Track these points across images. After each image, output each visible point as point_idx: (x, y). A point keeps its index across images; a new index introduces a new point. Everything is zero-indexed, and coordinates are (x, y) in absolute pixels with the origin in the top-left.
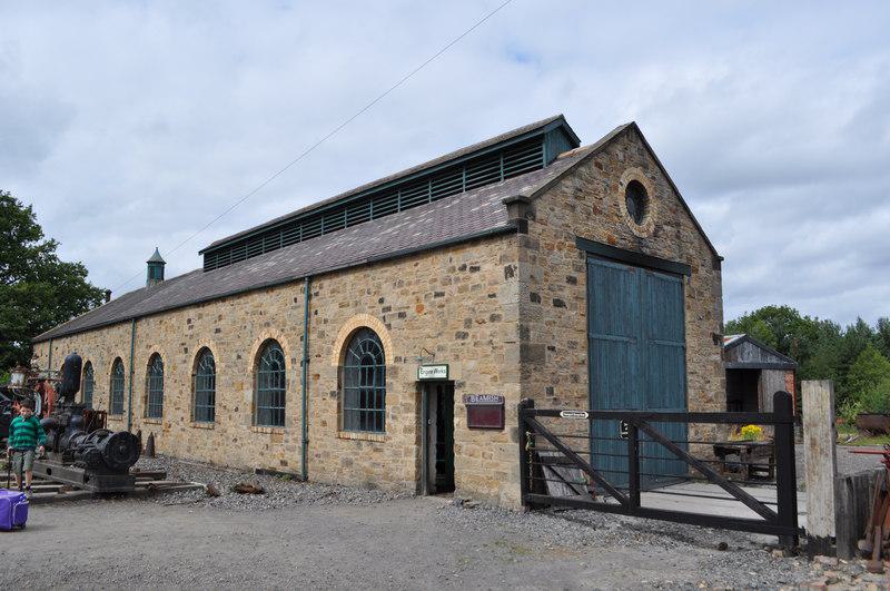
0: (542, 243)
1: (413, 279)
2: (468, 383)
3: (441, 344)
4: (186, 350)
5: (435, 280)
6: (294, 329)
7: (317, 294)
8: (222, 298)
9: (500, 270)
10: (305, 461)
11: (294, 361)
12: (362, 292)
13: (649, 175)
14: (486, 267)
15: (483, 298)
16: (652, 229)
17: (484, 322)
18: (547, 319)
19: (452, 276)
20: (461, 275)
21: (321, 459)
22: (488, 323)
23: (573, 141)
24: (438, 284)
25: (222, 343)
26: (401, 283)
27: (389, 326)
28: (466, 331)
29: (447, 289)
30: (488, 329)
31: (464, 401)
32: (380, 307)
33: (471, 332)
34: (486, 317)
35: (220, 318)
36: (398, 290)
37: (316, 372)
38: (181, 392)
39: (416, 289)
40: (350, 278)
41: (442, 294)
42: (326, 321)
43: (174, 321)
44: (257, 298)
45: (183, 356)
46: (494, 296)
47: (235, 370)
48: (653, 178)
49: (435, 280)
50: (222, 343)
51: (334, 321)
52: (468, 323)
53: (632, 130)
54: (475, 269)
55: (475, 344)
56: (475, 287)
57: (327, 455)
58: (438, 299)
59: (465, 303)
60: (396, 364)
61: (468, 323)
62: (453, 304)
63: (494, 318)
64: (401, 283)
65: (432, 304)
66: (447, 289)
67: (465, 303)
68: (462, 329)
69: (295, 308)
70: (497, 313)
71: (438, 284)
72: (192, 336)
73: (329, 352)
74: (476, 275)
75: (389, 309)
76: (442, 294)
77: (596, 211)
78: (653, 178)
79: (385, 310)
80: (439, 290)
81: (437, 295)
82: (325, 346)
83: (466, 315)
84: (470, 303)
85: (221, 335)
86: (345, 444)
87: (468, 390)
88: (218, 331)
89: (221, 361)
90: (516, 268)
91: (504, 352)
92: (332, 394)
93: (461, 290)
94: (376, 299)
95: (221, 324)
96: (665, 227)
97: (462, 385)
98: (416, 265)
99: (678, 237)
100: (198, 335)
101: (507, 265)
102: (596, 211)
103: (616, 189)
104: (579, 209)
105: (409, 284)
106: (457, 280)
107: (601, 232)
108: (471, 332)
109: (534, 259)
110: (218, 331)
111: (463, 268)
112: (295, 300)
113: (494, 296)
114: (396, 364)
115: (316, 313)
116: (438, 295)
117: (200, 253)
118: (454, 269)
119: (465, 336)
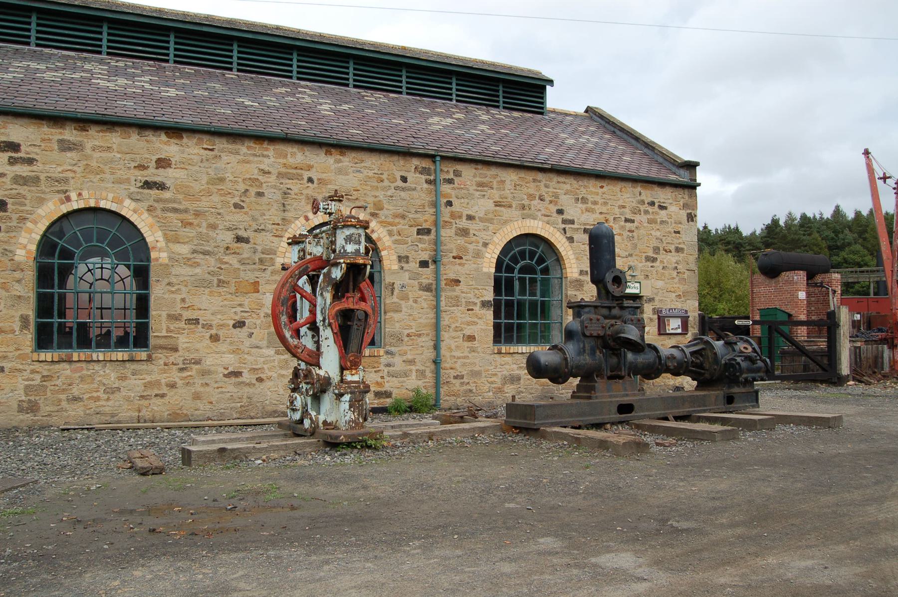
1: (597, 198)
2: (657, 299)
3: (631, 264)
5: (624, 207)
6: (403, 217)
7: (450, 181)
8: (175, 131)
9: (683, 214)
10: (437, 385)
11: (403, 259)
12: (531, 197)
14: (673, 209)
15: (670, 232)
17: (670, 252)
19: (642, 208)
20: (650, 209)
21: (465, 380)
22: (673, 253)
24: (627, 210)
25: (175, 210)
27: (571, 240)
28: (655, 256)
29: (637, 218)
30: (673, 258)
31: (654, 314)
32: (560, 218)
33: (659, 257)
34: (672, 248)
35: (163, 163)
36: (580, 205)
37: (452, 276)
39: (604, 210)
40: (511, 177)
41: (633, 221)
42: (470, 218)
44: (297, 156)
46: (678, 232)
47: (233, 260)
49: (624, 207)
50: (175, 210)
51: (490, 221)
52: (656, 250)
54: (662, 208)
55: (663, 268)
56: (662, 222)
57: (476, 374)
58: (628, 225)
59: (653, 233)
60: (582, 278)
61: (656, 250)
62: (642, 232)
63: (678, 250)
64: (584, 200)
65: (623, 227)
66: (637, 218)
67: (653, 233)
68: (651, 254)
69: (403, 189)
70: (680, 246)
71: (627, 210)
73: (478, 255)
74: (663, 213)
75: (572, 222)
76: (633, 221)
79: (564, 222)
80: (628, 217)
81: (627, 220)
82: (471, 247)
83: (655, 243)
84: (658, 234)
85: (167, 195)
86: (508, 359)
87: (657, 304)
89: (172, 239)
91: (685, 276)
92: (484, 304)
93: (650, 222)
94: (554, 209)
97: (651, 300)
98: (602, 187)
101: (689, 211)
105: (595, 203)
106: (646, 212)
108: (659, 257)
111: (652, 204)
112: (404, 179)
113: (678, 232)
114: (582, 278)
115: (450, 203)
116: (627, 220)
118: (643, 202)
119: (654, 260)
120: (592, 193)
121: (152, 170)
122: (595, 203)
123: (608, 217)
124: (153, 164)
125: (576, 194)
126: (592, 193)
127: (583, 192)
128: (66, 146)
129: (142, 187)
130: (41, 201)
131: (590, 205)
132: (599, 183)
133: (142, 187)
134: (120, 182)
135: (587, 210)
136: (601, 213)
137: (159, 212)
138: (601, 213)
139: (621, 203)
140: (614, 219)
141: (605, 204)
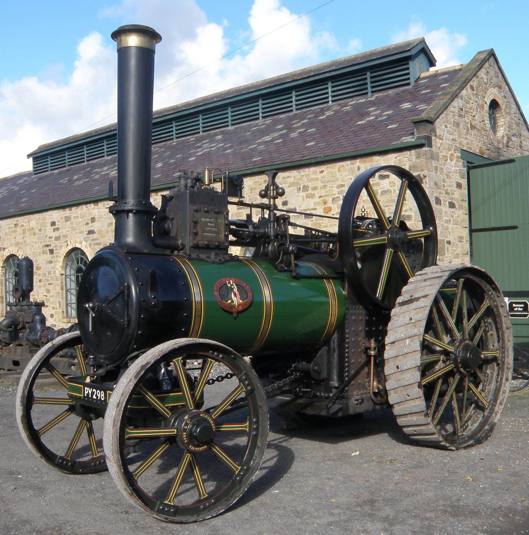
0: (441, 155)
1: (319, 184)
4: (52, 252)
13: (503, 94)
16: (505, 140)
18: (445, 218)
23: (432, 62)
26: (306, 188)
35: (93, 220)
36: (304, 194)
38: (48, 291)
39: (323, 192)
43: (33, 224)
45: (48, 257)
48: (505, 97)
53: (492, 54)
64: (306, 188)
72: (58, 238)
77: (473, 127)
78: (505, 97)
85: (95, 236)
88: (91, 232)
90: (425, 177)
95: (95, 226)
96: (513, 138)
98: (322, 172)
99: (521, 146)
100: (66, 236)
102: (473, 127)
103: (483, 107)
104: (461, 125)
105: (315, 188)
107: (475, 144)
109: (436, 168)
110: (91, 232)
117: (29, 156)
120: (312, 180)
121: (90, 224)
122: (315, 188)
123: (326, 198)
124: (90, 221)
125: (298, 184)
126: (312, 180)
127: (305, 182)
128: (67, 219)
129: (88, 234)
130: (61, 247)
131: (310, 191)
132: (318, 169)
133: (88, 234)
134: (81, 232)
135: (308, 196)
136: (320, 197)
137: (93, 246)
138: (320, 197)
139: (339, 182)
140: (333, 199)
141: (325, 187)
